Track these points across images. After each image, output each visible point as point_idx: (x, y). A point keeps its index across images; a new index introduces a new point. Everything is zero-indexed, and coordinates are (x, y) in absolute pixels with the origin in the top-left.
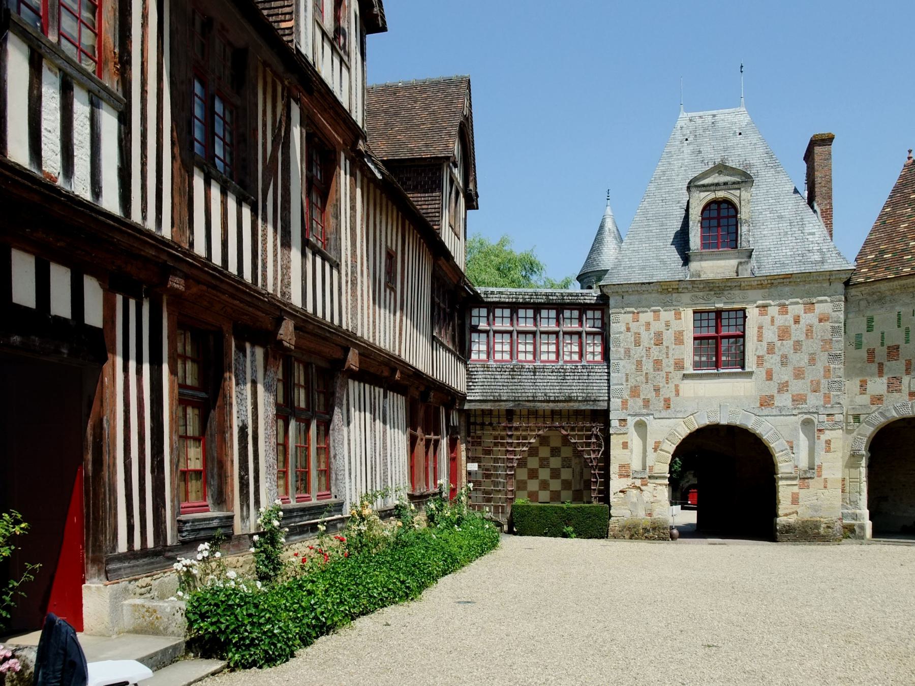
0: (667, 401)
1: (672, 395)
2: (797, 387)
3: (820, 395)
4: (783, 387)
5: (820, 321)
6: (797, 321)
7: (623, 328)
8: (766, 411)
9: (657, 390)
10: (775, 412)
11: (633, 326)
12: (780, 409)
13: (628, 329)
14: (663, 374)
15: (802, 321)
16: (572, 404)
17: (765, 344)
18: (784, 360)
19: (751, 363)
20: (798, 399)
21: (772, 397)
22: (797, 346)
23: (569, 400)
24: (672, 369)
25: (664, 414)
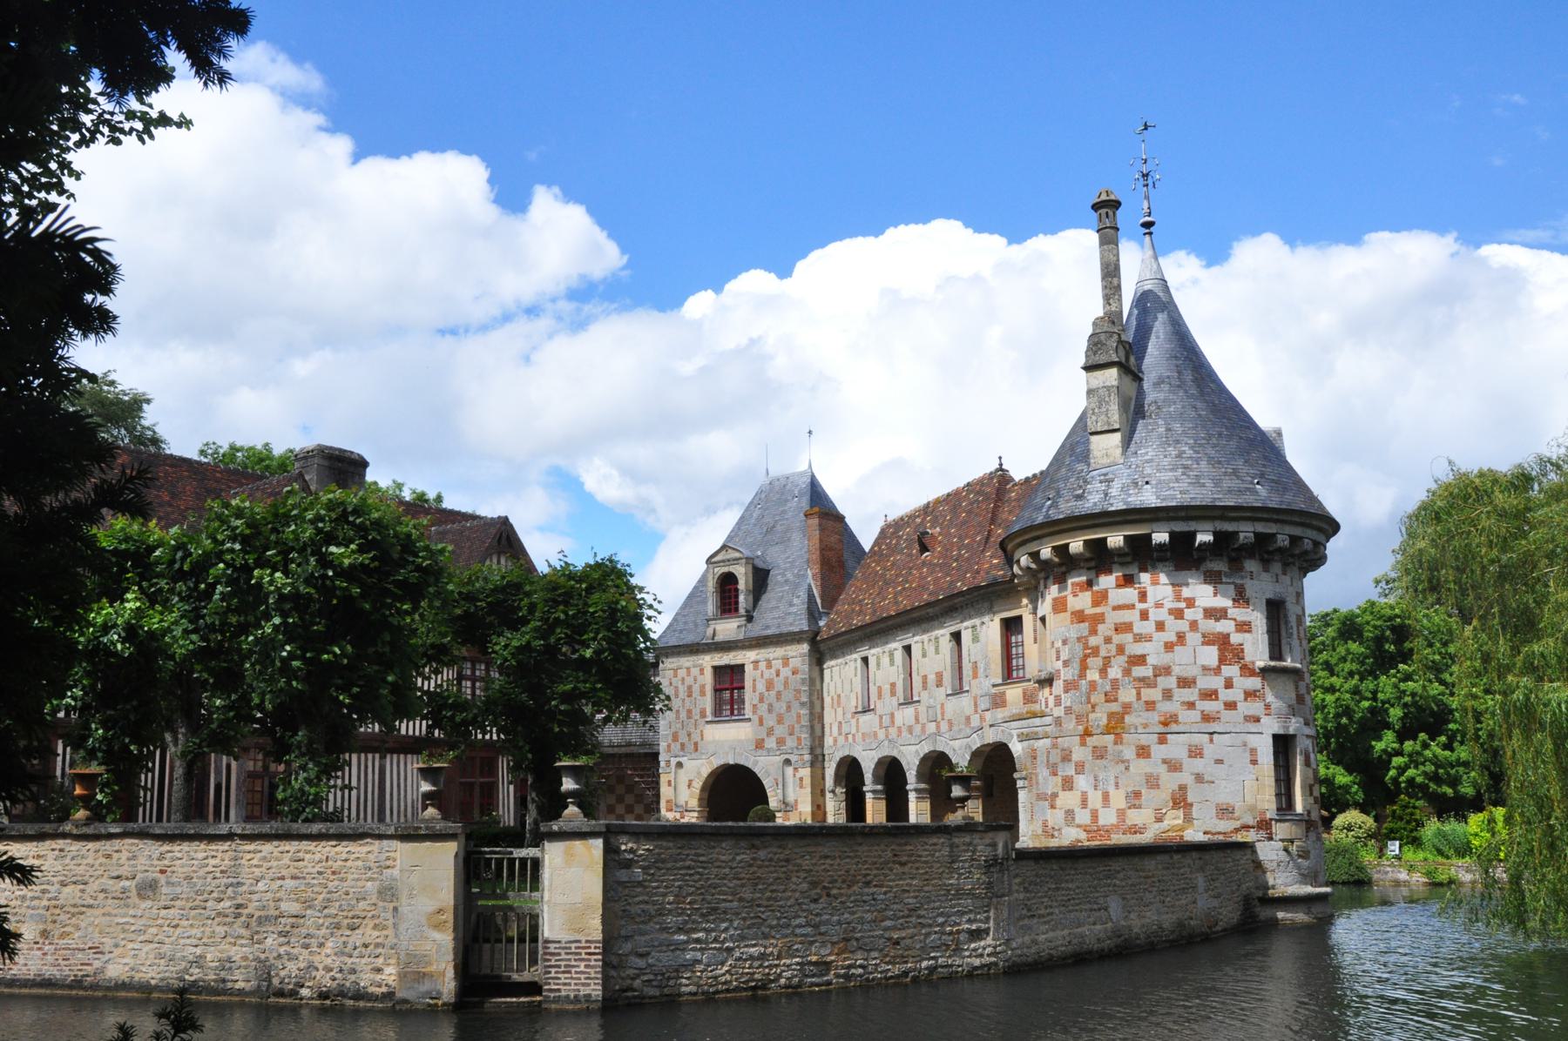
0: (696, 744)
1: (698, 739)
2: (780, 731)
3: (795, 737)
4: (770, 732)
5: (793, 674)
6: (778, 675)
7: (668, 683)
8: (759, 753)
9: (689, 735)
10: (765, 753)
11: (674, 680)
12: (769, 750)
13: (671, 684)
14: (693, 721)
15: (781, 674)
16: (632, 748)
17: (757, 693)
18: (770, 709)
19: (748, 712)
20: (781, 742)
21: (763, 740)
22: (779, 694)
23: (629, 744)
24: (698, 717)
25: (694, 756)
